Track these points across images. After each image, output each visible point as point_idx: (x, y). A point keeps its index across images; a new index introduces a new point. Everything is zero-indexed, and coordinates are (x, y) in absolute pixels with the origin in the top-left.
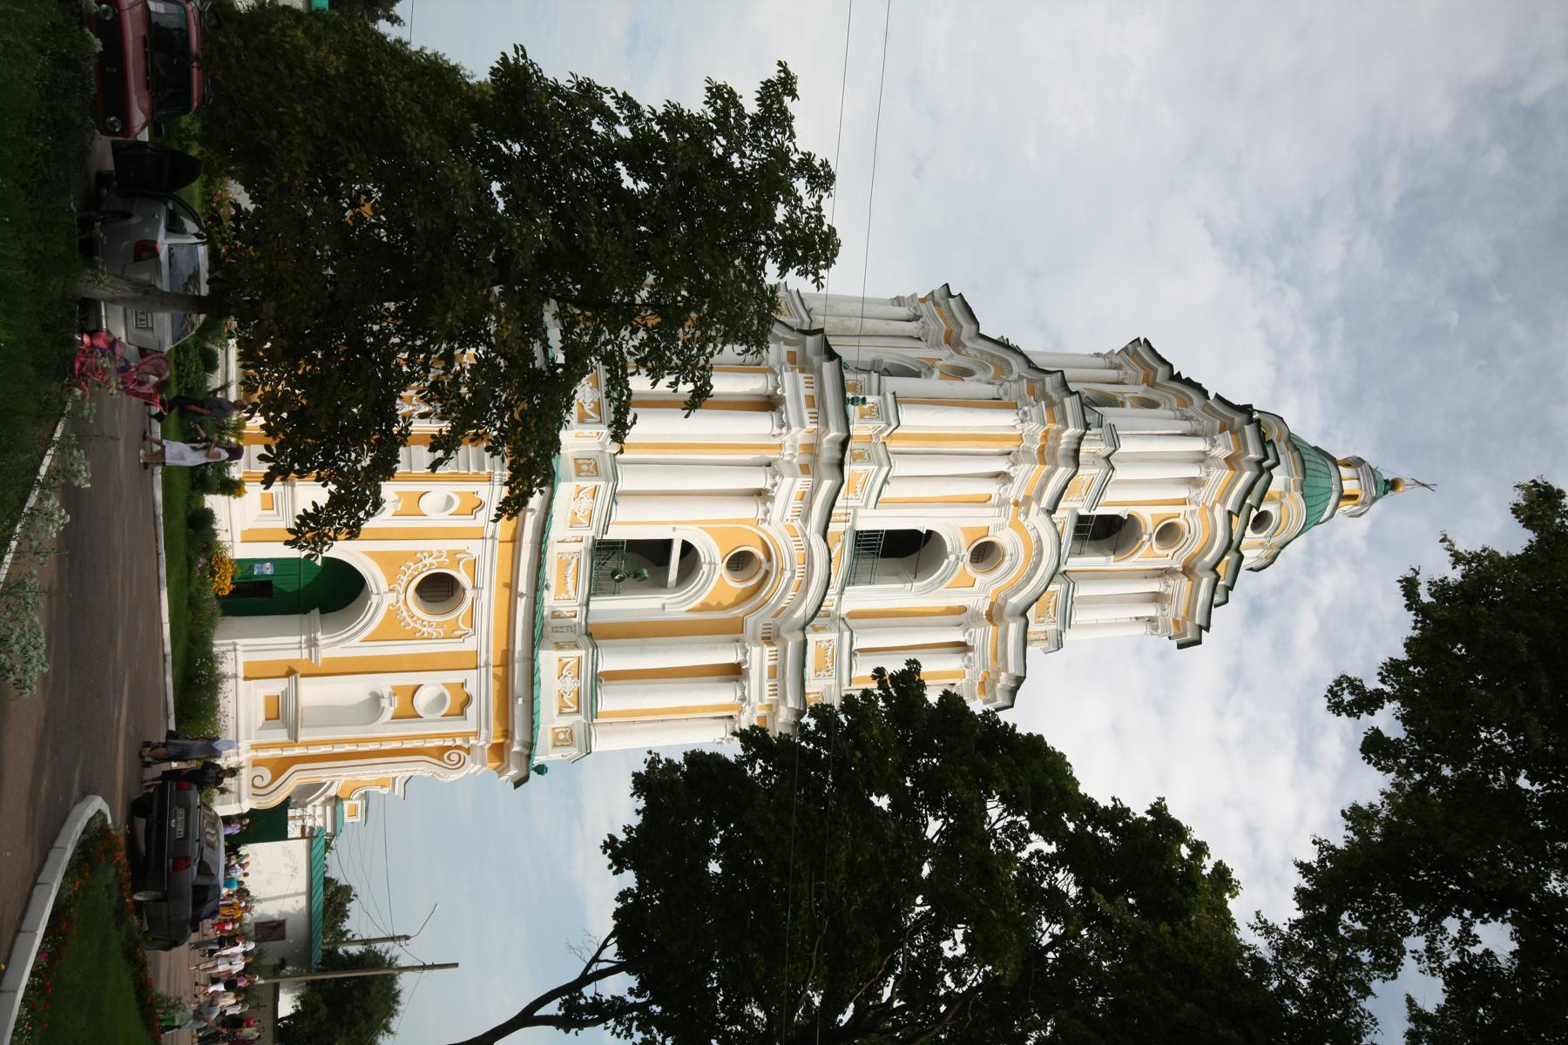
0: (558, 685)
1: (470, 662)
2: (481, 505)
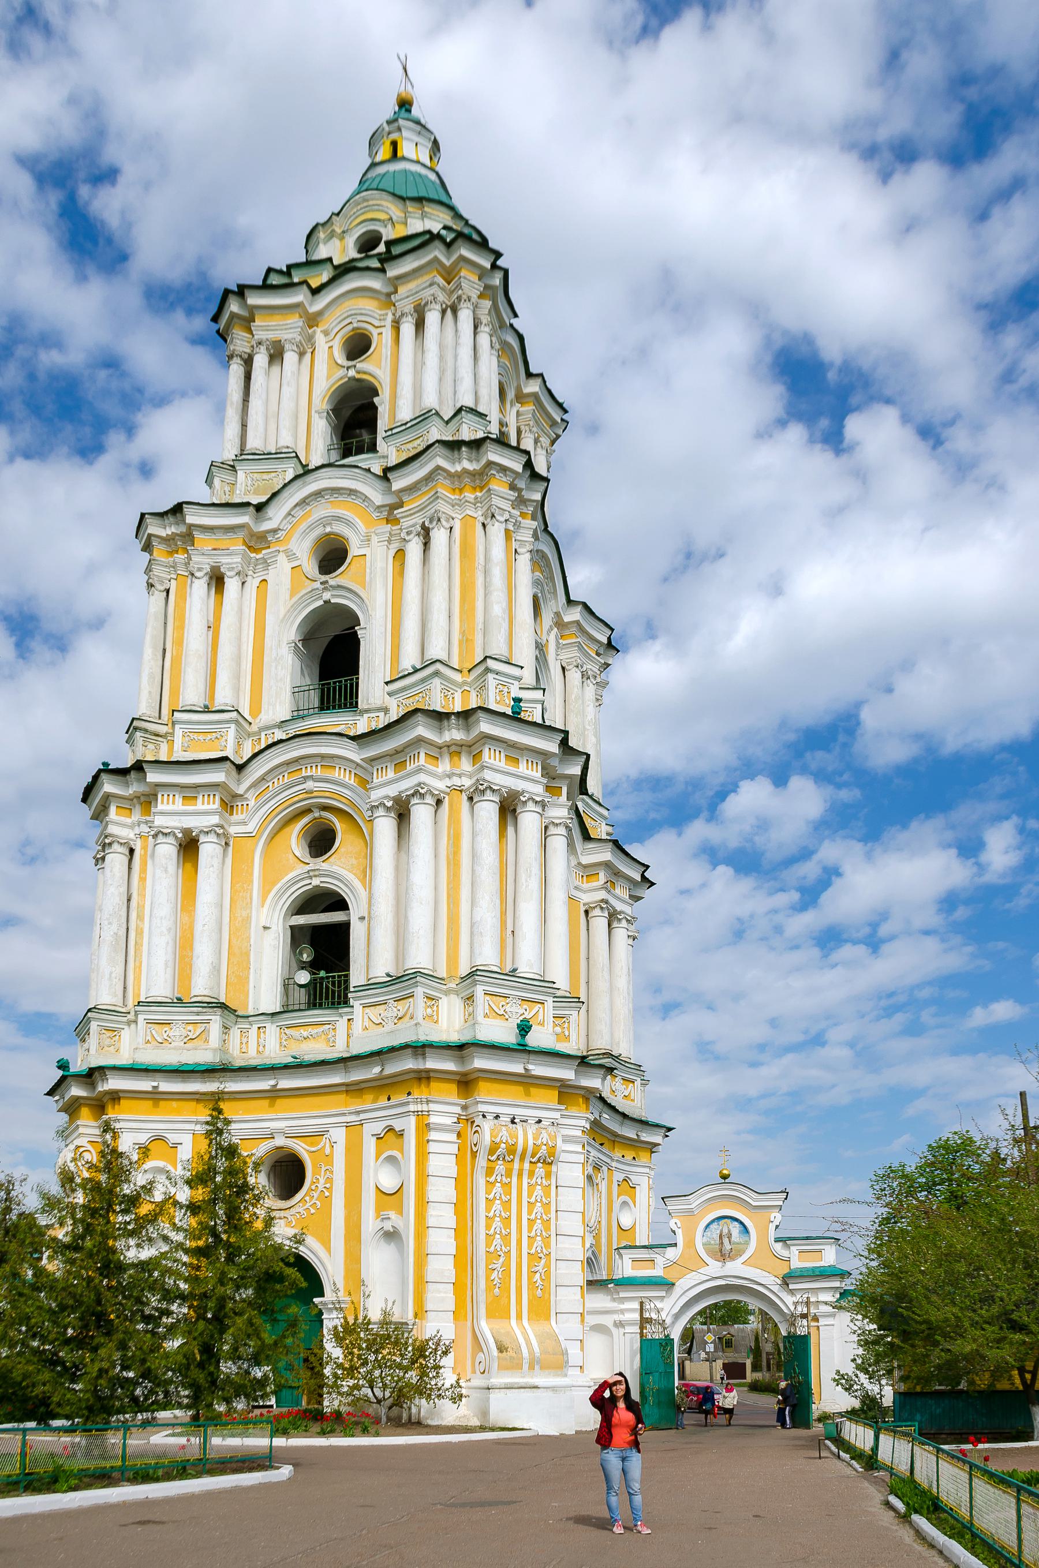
0: (390, 1026)
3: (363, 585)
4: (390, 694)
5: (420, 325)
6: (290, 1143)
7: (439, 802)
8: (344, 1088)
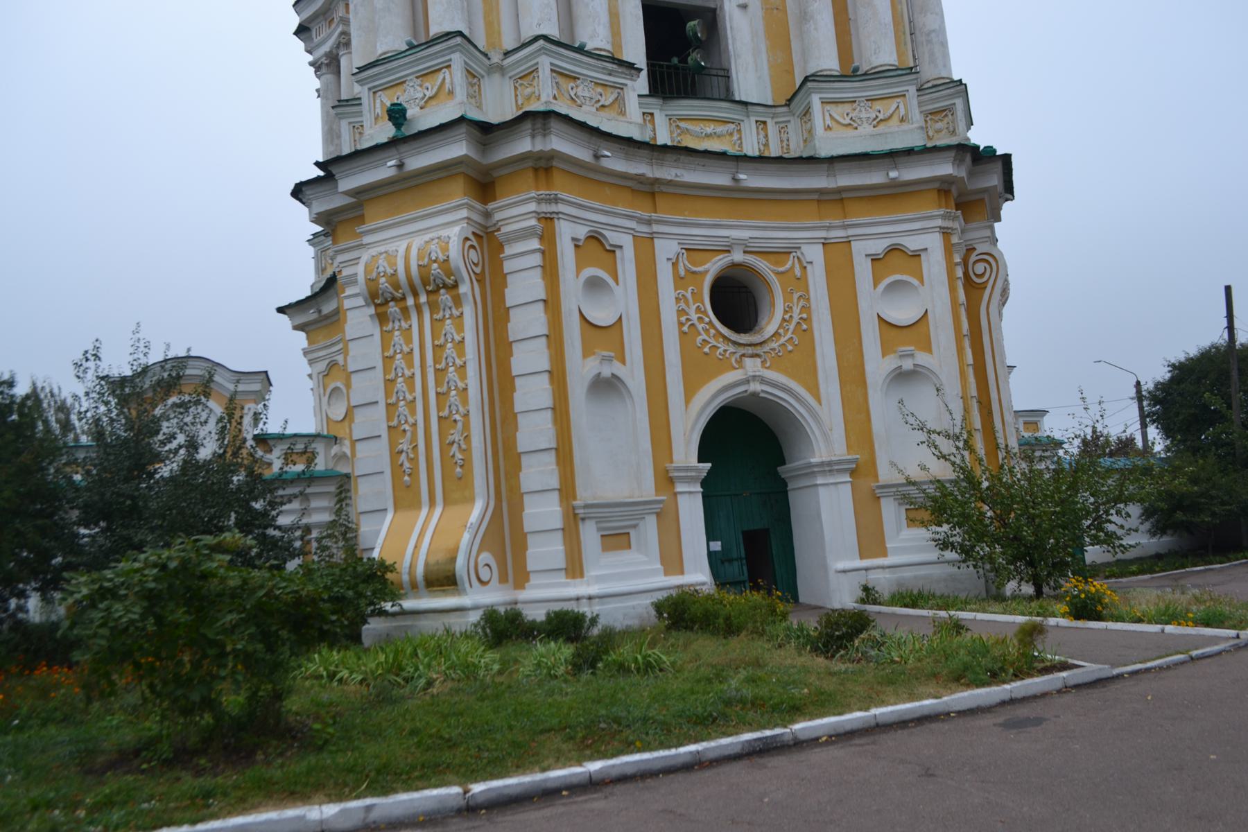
0: (866, 129)
1: (838, 254)
2: (595, 238)
6: (751, 259)
8: (816, 197)
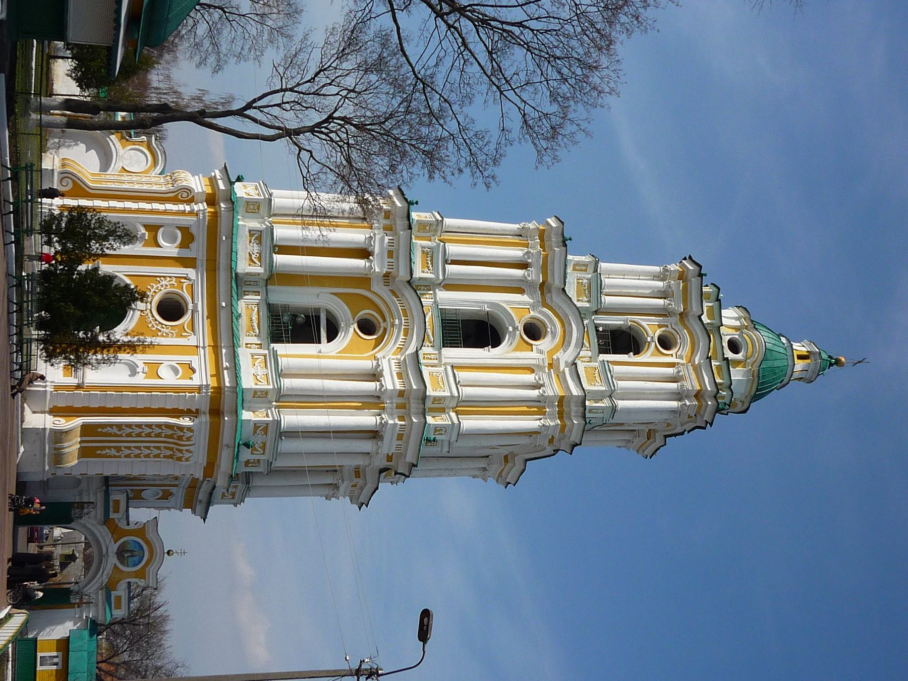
3: (516, 349)
4: (446, 369)
5: (674, 379)
6: (190, 312)
7: (379, 397)
